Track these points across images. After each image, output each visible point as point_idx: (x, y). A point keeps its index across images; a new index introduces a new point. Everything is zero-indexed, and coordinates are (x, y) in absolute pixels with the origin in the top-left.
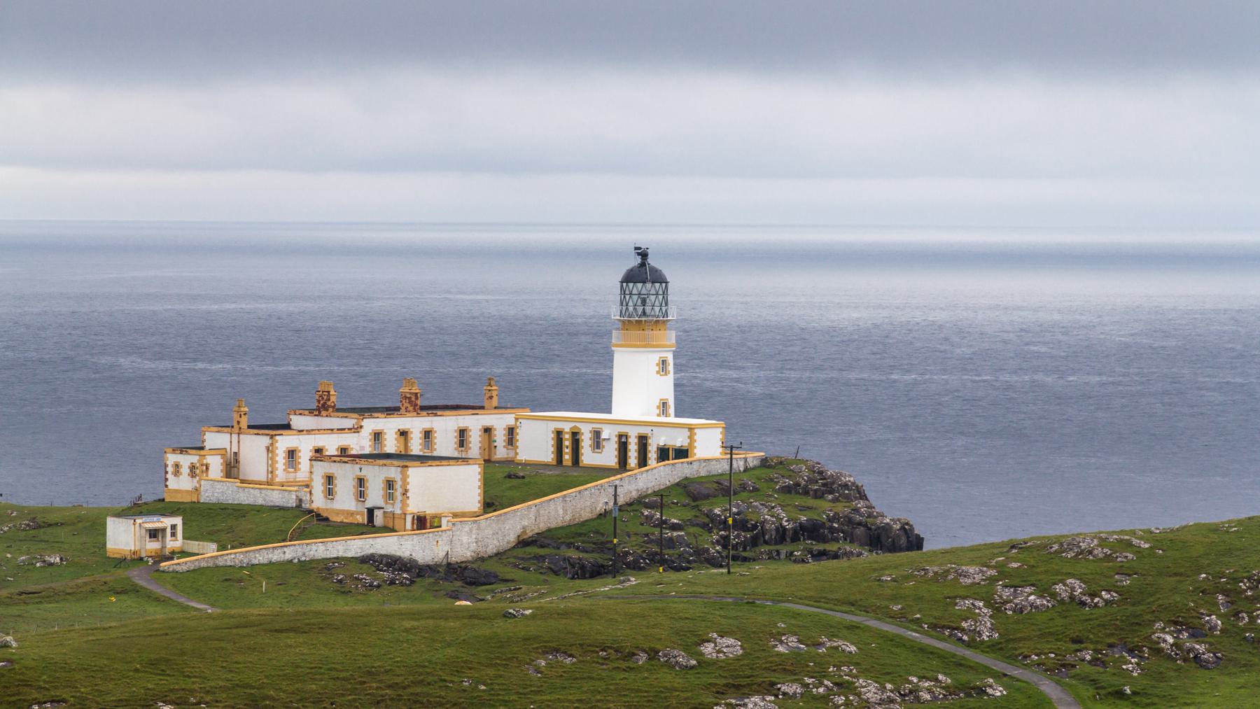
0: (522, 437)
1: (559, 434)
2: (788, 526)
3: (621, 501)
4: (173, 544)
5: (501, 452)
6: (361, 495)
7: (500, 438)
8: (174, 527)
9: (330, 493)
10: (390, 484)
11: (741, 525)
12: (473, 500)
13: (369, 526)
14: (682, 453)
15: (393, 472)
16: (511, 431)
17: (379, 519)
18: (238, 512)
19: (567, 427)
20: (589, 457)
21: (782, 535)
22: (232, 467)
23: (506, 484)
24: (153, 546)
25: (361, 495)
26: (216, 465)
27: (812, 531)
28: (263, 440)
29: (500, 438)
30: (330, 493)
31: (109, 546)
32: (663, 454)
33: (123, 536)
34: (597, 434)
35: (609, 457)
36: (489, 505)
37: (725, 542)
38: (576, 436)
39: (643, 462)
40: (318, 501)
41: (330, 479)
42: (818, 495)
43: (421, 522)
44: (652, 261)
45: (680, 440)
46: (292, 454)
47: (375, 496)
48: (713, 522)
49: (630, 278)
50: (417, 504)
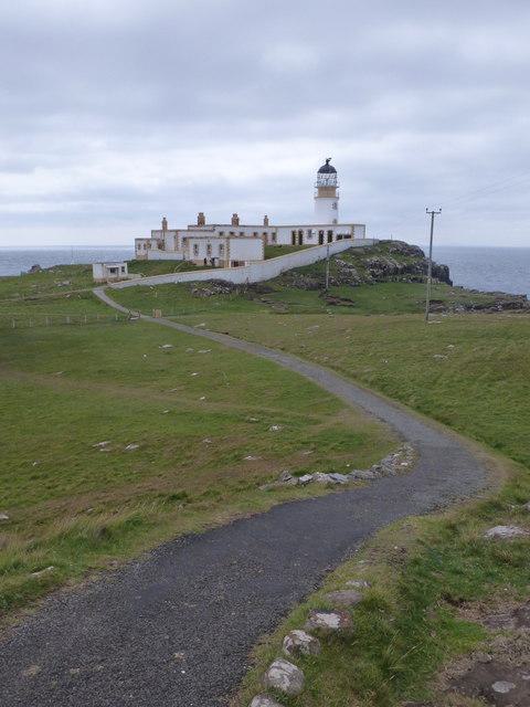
0: (278, 236)
1: (294, 233)
2: (400, 267)
3: (330, 254)
4: (121, 275)
5: (270, 243)
6: (209, 253)
7: (270, 237)
8: (123, 268)
9: (196, 252)
10: (221, 247)
11: (380, 267)
12: (260, 253)
13: (210, 265)
14: (348, 237)
15: (223, 241)
16: (274, 234)
17: (216, 264)
18: (160, 262)
19: (297, 230)
20: (306, 241)
21: (396, 271)
22: (161, 246)
23: (271, 252)
24: (114, 276)
25: (209, 253)
26: (154, 244)
27: (408, 269)
28: (174, 234)
29: (270, 237)
30: (196, 252)
31: (95, 276)
32: (339, 237)
33: (98, 273)
34: (310, 232)
35: (315, 240)
36: (267, 257)
37: (373, 274)
38: (300, 233)
39: (330, 240)
40: (191, 257)
41: (196, 246)
42: (407, 254)
43: (236, 264)
44: (330, 163)
45: (347, 231)
46: (184, 239)
47: (215, 253)
48: (364, 267)
49: (323, 170)
50: (234, 256)
